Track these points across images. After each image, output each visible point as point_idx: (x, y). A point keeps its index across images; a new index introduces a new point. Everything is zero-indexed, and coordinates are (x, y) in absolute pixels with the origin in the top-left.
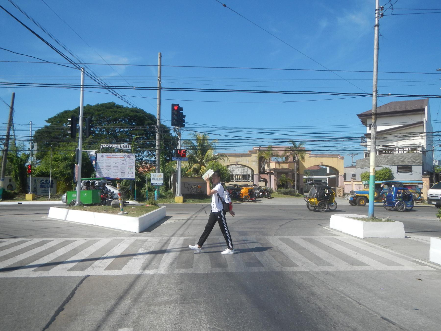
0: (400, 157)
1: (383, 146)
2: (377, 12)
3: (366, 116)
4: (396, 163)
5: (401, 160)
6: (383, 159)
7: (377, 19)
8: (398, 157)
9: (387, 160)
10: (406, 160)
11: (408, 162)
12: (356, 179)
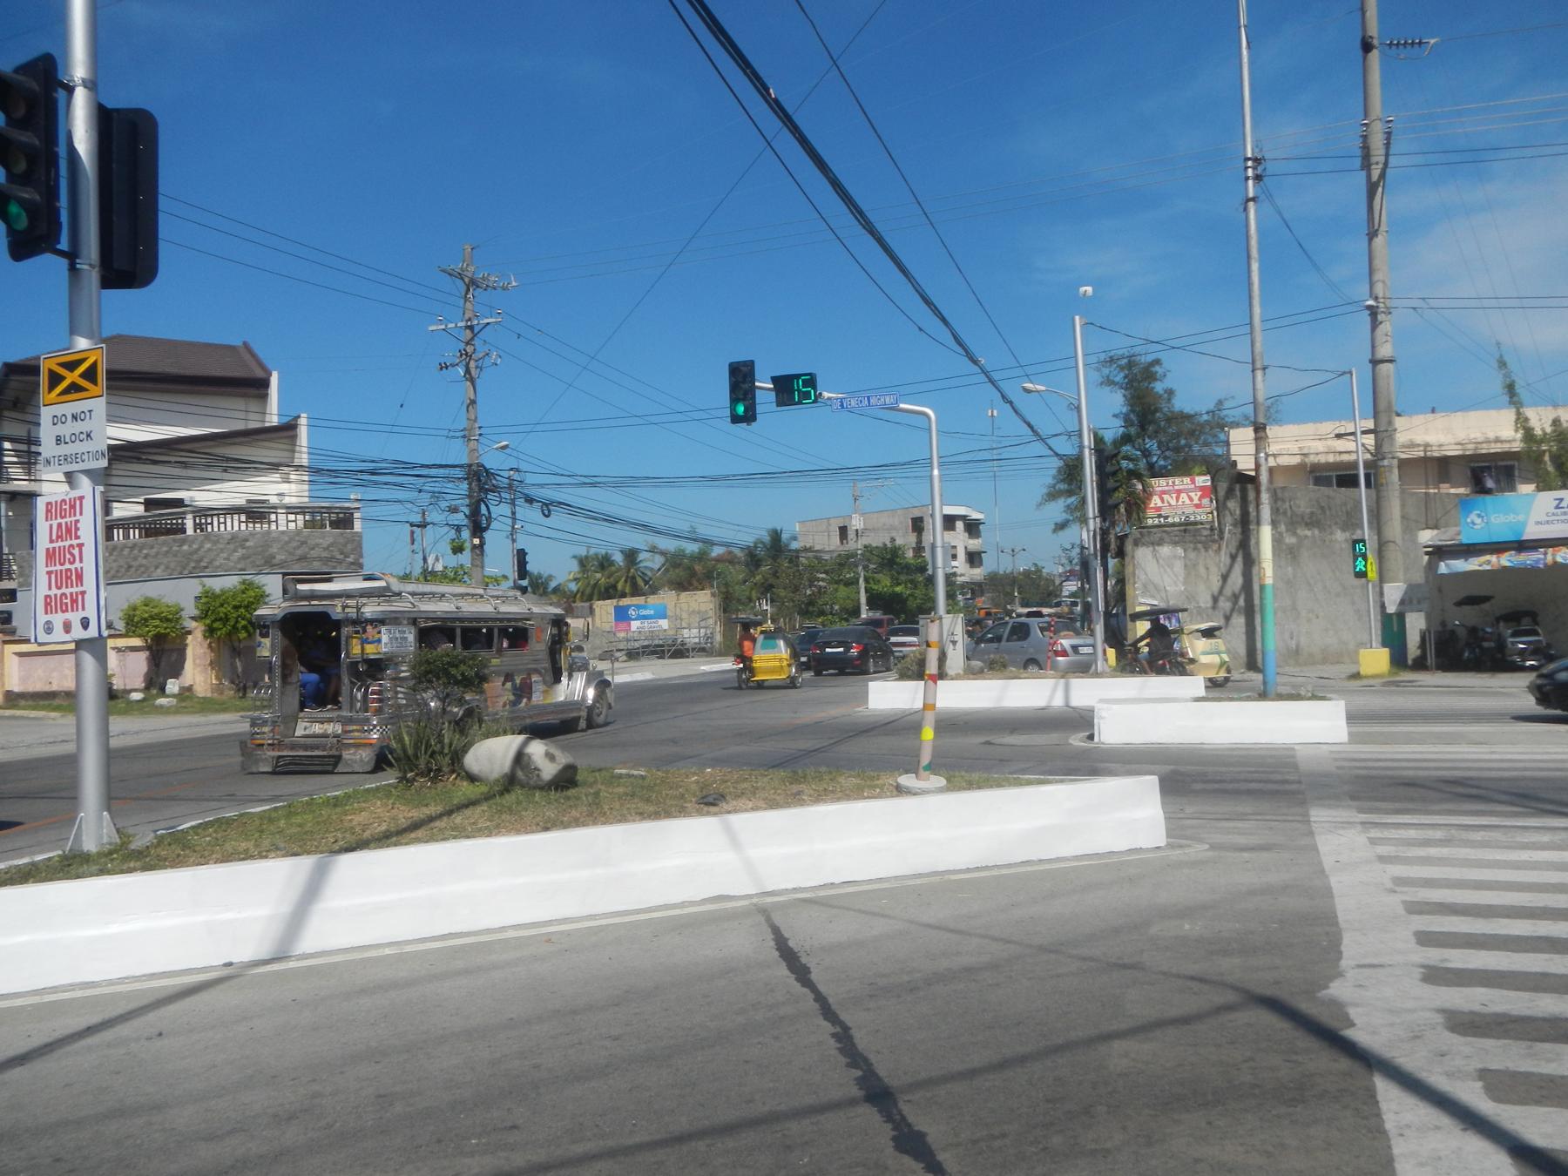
0: (295, 544)
1: (149, 504)
2: (1250, 163)
3: (121, 379)
4: (281, 564)
5: (299, 552)
6: (222, 550)
7: (1250, 182)
8: (287, 543)
9: (241, 552)
10: (314, 553)
11: (320, 559)
12: (13, 632)
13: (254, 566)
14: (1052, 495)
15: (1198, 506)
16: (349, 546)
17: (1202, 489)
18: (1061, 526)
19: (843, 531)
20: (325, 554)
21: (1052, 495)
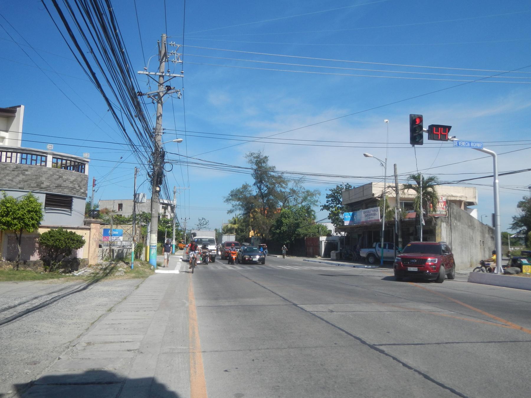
9: (21, 177)
13: (30, 186)
14: (228, 200)
15: (443, 208)
16: (83, 183)
17: (444, 202)
18: (231, 212)
19: (120, 206)
20: (71, 185)
21: (228, 200)
